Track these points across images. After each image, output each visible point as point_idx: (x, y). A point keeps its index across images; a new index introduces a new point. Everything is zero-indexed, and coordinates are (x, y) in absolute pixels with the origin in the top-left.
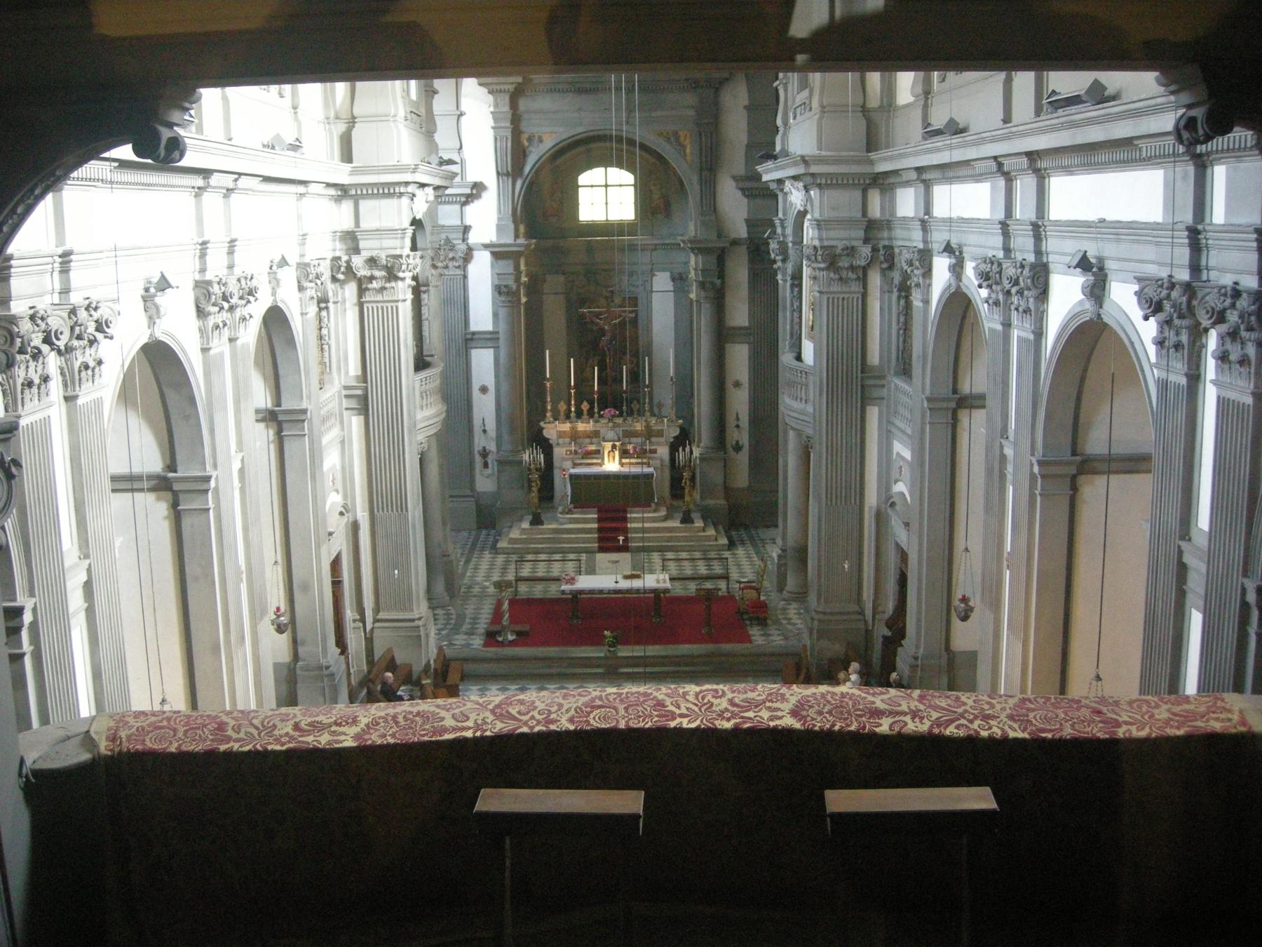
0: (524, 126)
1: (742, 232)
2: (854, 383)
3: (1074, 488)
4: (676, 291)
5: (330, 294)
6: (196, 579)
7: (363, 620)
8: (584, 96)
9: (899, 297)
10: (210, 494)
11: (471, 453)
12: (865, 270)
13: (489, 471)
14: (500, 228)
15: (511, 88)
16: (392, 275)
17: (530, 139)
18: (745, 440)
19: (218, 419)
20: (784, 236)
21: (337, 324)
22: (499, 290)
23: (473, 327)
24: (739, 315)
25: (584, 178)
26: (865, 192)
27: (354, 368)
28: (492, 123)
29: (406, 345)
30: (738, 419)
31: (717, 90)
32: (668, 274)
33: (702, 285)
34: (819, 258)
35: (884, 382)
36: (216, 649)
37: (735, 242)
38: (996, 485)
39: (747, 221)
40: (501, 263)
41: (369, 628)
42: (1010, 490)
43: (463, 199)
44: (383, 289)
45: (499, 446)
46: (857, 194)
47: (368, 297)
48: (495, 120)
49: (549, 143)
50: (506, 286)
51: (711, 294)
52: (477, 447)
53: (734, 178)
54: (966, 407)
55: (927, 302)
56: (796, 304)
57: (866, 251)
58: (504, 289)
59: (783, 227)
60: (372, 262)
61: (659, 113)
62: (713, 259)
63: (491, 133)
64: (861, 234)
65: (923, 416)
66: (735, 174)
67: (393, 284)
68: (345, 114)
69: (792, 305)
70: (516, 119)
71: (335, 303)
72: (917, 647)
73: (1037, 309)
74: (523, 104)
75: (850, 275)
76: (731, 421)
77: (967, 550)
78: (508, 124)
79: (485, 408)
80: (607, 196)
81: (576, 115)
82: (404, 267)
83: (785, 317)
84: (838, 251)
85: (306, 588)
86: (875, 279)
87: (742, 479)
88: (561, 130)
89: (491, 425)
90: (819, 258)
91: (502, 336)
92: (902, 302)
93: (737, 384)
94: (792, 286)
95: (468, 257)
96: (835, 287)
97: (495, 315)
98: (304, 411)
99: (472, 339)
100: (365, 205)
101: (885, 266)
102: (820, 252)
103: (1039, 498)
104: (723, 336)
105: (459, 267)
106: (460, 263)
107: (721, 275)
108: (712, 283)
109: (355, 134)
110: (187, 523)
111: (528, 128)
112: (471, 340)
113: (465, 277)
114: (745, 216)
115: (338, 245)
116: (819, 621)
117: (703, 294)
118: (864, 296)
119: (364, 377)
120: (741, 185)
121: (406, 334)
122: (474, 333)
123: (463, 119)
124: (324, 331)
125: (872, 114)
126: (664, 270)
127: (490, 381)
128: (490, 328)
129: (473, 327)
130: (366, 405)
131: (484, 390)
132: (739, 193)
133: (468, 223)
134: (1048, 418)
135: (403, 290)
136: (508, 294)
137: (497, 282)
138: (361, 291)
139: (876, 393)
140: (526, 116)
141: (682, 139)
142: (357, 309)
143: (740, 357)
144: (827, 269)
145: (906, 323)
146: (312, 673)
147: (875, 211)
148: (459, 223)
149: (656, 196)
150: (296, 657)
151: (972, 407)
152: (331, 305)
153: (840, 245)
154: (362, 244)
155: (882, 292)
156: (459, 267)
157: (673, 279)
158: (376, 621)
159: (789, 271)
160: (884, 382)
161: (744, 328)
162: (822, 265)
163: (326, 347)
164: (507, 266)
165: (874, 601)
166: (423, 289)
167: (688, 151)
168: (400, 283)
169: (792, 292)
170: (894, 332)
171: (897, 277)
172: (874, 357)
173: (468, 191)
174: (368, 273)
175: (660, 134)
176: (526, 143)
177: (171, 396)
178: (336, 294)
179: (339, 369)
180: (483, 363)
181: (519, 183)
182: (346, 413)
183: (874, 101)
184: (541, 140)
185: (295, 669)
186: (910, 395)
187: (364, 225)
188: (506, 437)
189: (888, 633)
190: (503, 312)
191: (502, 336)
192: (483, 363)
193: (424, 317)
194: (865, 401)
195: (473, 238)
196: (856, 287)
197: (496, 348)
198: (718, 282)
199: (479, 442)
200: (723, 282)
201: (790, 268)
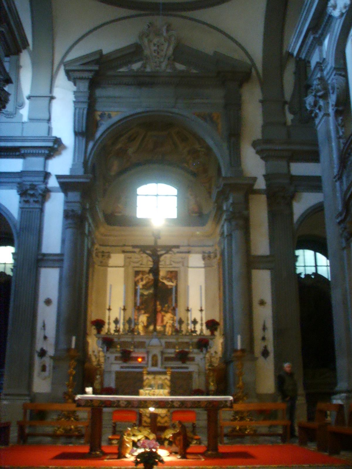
1: (261, 184)
4: (206, 266)
13: (46, 374)
15: (90, 75)
17: (102, 116)
18: (271, 348)
22: (67, 215)
23: (45, 249)
30: (264, 328)
32: (199, 256)
37: (258, 192)
39: (264, 176)
40: (70, 194)
43: (47, 152)
45: (56, 350)
48: (76, 97)
49: (116, 117)
50: (73, 211)
52: (38, 348)
53: (255, 144)
58: (71, 213)
61: (198, 101)
66: (254, 138)
69: (337, 132)
74: (99, 92)
76: (258, 333)
78: (86, 100)
89: (51, 331)
91: (66, 258)
93: (262, 303)
95: (46, 194)
97: (63, 241)
99: (42, 260)
106: (40, 199)
111: (100, 108)
113: (42, 210)
120: (259, 148)
122: (44, 255)
123: (54, 102)
127: (54, 295)
129: (45, 249)
131: (48, 302)
132: (258, 157)
133: (50, 170)
137: (66, 208)
156: (36, 202)
157: (204, 258)
161: (267, 257)
164: (75, 196)
173: (50, 144)
176: (98, 118)
184: (110, 117)
190: (69, 232)
191: (66, 258)
195: (53, 183)
197: (61, 267)
199: (39, 345)
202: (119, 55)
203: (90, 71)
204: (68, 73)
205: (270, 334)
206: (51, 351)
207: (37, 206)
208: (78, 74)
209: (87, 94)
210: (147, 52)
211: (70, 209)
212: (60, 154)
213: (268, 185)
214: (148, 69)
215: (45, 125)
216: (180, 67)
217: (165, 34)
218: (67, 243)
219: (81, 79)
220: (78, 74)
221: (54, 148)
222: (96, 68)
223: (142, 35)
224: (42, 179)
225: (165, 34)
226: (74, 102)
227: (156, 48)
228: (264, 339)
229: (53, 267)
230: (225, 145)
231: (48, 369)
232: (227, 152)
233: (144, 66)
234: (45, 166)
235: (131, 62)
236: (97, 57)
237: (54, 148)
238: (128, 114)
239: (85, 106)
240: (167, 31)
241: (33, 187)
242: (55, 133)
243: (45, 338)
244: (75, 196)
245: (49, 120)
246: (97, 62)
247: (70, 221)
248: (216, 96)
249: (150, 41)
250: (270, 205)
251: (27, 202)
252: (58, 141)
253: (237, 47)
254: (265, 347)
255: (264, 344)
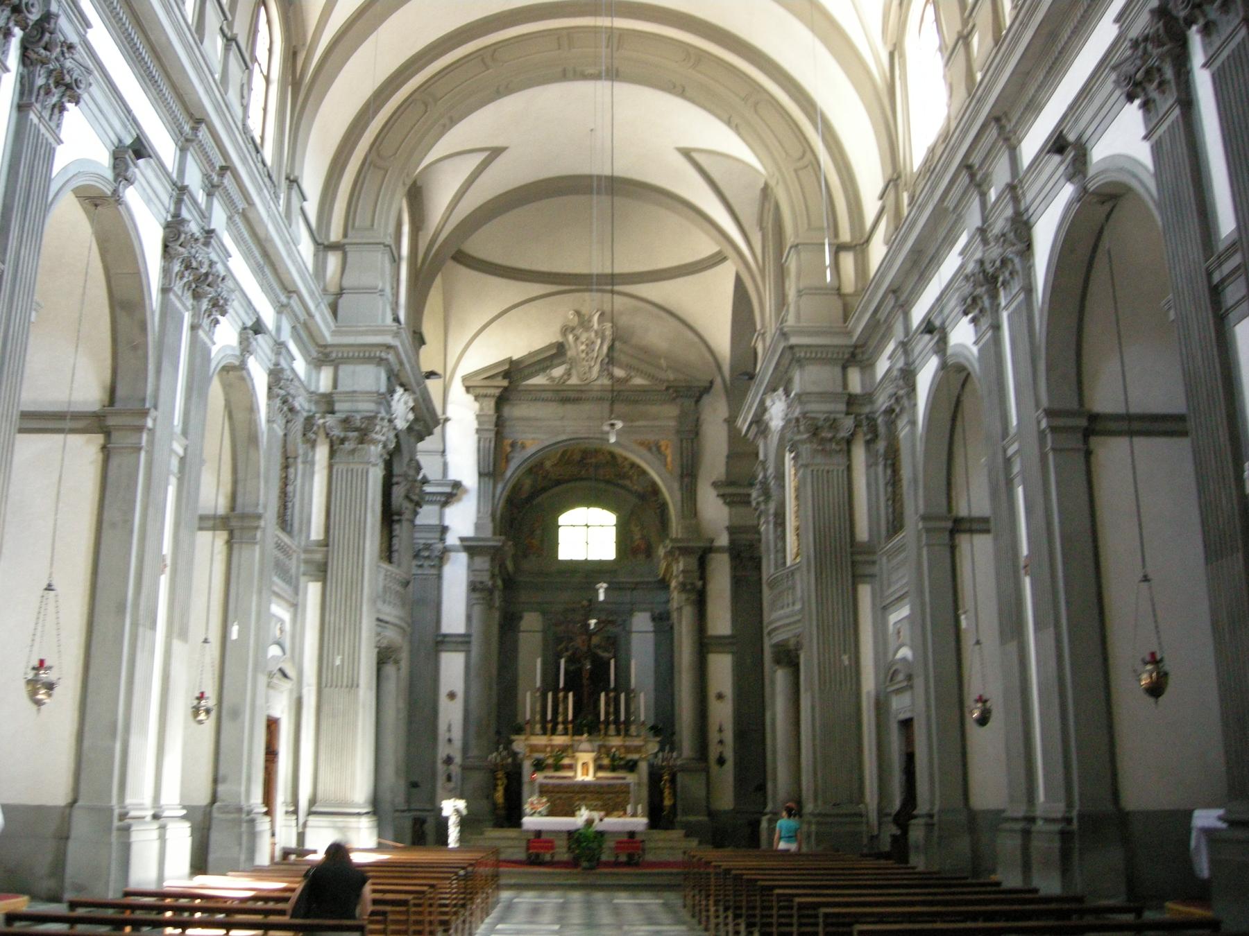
0: (507, 431)
1: (723, 540)
2: (846, 561)
3: (1088, 454)
4: (657, 631)
5: (301, 452)
6: (113, 525)
7: (296, 812)
8: (569, 407)
9: (885, 465)
10: (143, 455)
11: (434, 763)
12: (849, 442)
13: (452, 785)
14: (478, 527)
15: (497, 392)
16: (364, 435)
17: (513, 445)
18: (729, 754)
19: (166, 366)
20: (765, 477)
21: (303, 485)
22: (473, 587)
24: (721, 622)
25: (563, 519)
26: (844, 368)
27: (316, 533)
28: (475, 425)
29: (373, 511)
30: (720, 730)
31: (698, 401)
33: (683, 587)
34: (802, 428)
35: (875, 558)
36: (121, 609)
37: (720, 550)
38: (1004, 497)
41: (301, 821)
42: (1020, 491)
43: (443, 499)
44: (353, 451)
46: (837, 370)
47: (337, 459)
48: (480, 423)
49: (531, 449)
50: (481, 583)
51: (693, 597)
53: (715, 485)
54: (965, 531)
55: (913, 423)
56: (780, 545)
57: (849, 422)
59: (765, 470)
60: (346, 422)
62: (693, 562)
63: (475, 437)
64: (842, 407)
65: (919, 540)
66: (714, 478)
67: (365, 446)
68: (333, 288)
70: (500, 425)
71: (304, 462)
72: (932, 803)
73: (1023, 269)
74: (507, 411)
75: (834, 446)
76: (714, 736)
77: (978, 643)
78: (492, 427)
79: (451, 715)
80: (587, 534)
81: (558, 423)
82: (378, 428)
83: (769, 560)
84: (820, 423)
85: (236, 714)
86: (859, 454)
87: (725, 800)
88: (543, 437)
89: (457, 734)
90: (802, 428)
92: (889, 472)
93: (720, 696)
94: (776, 524)
95: (441, 558)
96: (819, 459)
97: (469, 618)
98: (259, 517)
99: (442, 642)
100: (345, 370)
101: (868, 437)
102: (802, 422)
103: (1051, 456)
104: (704, 645)
105: (433, 566)
106: (436, 562)
107: (703, 577)
108: (692, 584)
109: (343, 302)
110: (114, 462)
112: (442, 642)
113: (439, 577)
114: (727, 524)
115: (313, 408)
116: (818, 823)
117: (684, 596)
118: (849, 468)
119: (325, 543)
121: (374, 500)
122: (445, 636)
123: (449, 424)
124: (290, 488)
125: (848, 299)
126: (644, 610)
127: (459, 688)
128: (461, 629)
130: (325, 571)
132: (720, 502)
133: (447, 523)
134: (1050, 368)
135: (375, 452)
136: (482, 590)
138: (332, 453)
139: (868, 570)
140: (508, 423)
141: (663, 448)
142: (325, 472)
143: (722, 667)
144: (809, 440)
145: (894, 493)
146: (232, 816)
147: (855, 382)
148: (437, 523)
149: (637, 536)
150: (214, 799)
151: (971, 531)
152: (300, 460)
153: (822, 417)
154: (338, 407)
155: (869, 466)
156: (433, 566)
157: (654, 619)
158: (310, 813)
159: (772, 511)
160: (875, 558)
162: (805, 436)
163: (290, 505)
165: (879, 804)
166: (396, 518)
167: (669, 459)
168: (373, 448)
169: (775, 531)
170: (882, 499)
171: (881, 445)
172: (862, 533)
173: (448, 490)
174: (342, 435)
175: (642, 444)
177: (123, 319)
178: (306, 454)
179: (301, 531)
180: (453, 668)
181: (500, 487)
182: (303, 579)
183: (849, 285)
184: (523, 447)
185: (210, 812)
186: (905, 565)
187: (340, 389)
188: (473, 742)
189: (895, 830)
190: (477, 609)
192: (453, 668)
193: (395, 548)
194: (856, 579)
195: (452, 539)
196: (840, 460)
197: (468, 652)
198: (700, 583)
199: (443, 751)
200: (704, 586)
201: (772, 507)
202: (536, 359)
203: (498, 387)
204: (468, 389)
205: (729, 736)
206: (458, 759)
207: (433, 571)
208: (479, 391)
209: (494, 419)
210: (569, 354)
211: (479, 579)
212: (460, 500)
213: (732, 541)
214: (574, 380)
215: (438, 458)
216: (619, 373)
217: (596, 326)
218: (475, 622)
219: (485, 396)
220: (479, 391)
221: (454, 492)
222: (505, 383)
223: (565, 330)
224: (438, 535)
225: (596, 326)
226: (478, 431)
227: (583, 347)
228: (721, 742)
229: (456, 651)
230: (676, 485)
231: (454, 779)
232: (678, 495)
233: (568, 373)
234: (441, 516)
235: (551, 367)
236: (506, 367)
237: (454, 492)
238: (547, 443)
239: (492, 435)
240: (599, 322)
241: (428, 547)
242: (453, 475)
243: (450, 740)
244: (483, 563)
245: (444, 452)
246: (506, 375)
247: (477, 595)
248: (668, 414)
249: (577, 338)
250: (734, 568)
251: (421, 566)
252: (457, 485)
253: (696, 339)
254: (721, 753)
255: (720, 748)
